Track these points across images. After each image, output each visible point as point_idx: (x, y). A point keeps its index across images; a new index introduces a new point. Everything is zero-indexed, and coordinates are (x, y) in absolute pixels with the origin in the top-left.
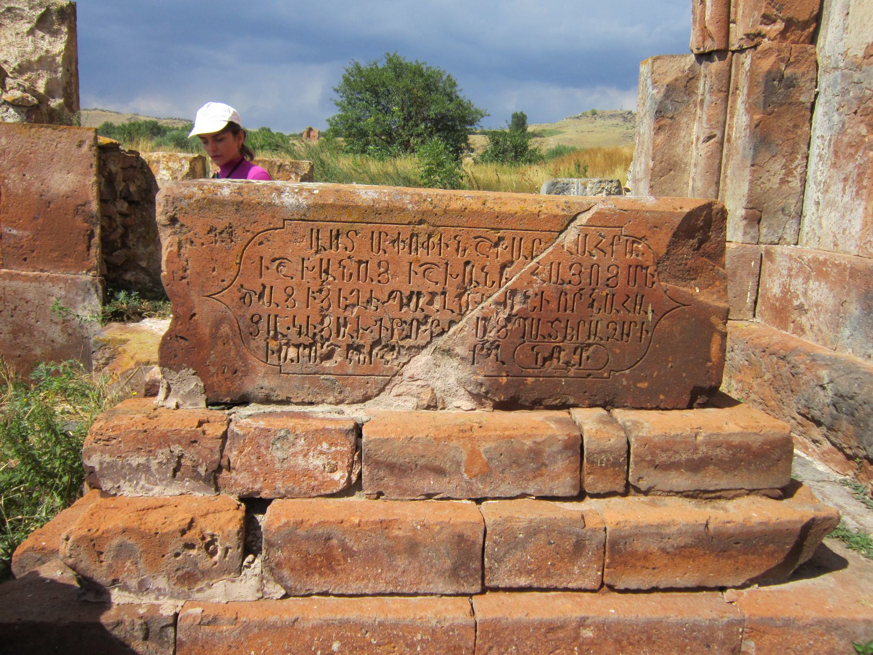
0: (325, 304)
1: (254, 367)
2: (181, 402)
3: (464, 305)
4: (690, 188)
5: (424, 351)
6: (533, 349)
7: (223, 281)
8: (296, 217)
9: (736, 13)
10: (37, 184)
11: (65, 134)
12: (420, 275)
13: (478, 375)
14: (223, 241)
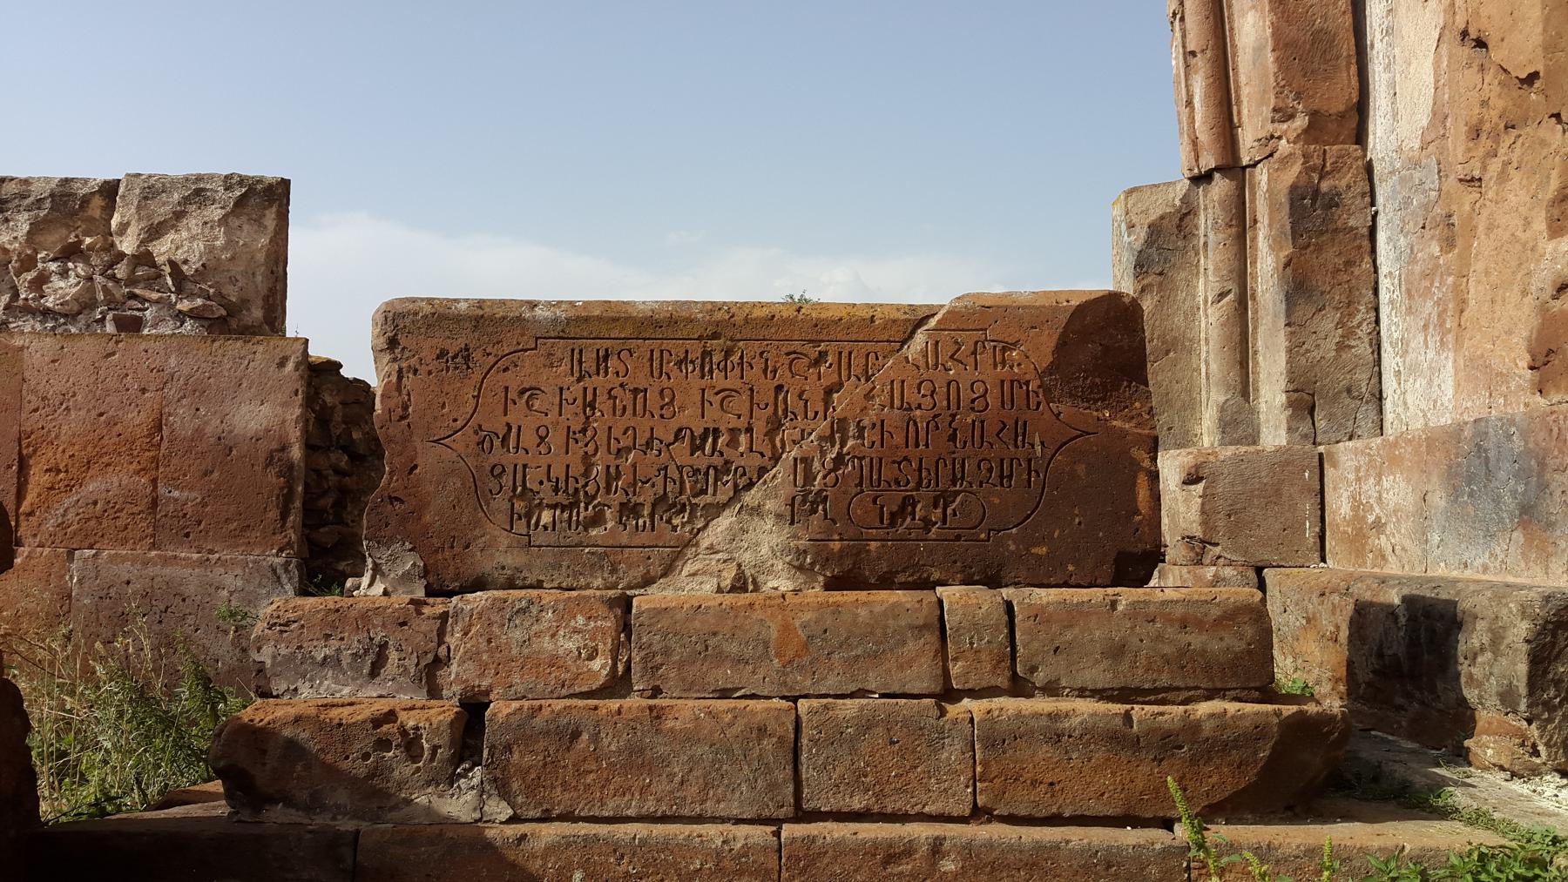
0: (591, 448)
3: (778, 444)
5: (727, 512)
6: (875, 502)
9: (1239, 113)
10: (215, 422)
11: (261, 348)
12: (716, 405)
13: (799, 539)
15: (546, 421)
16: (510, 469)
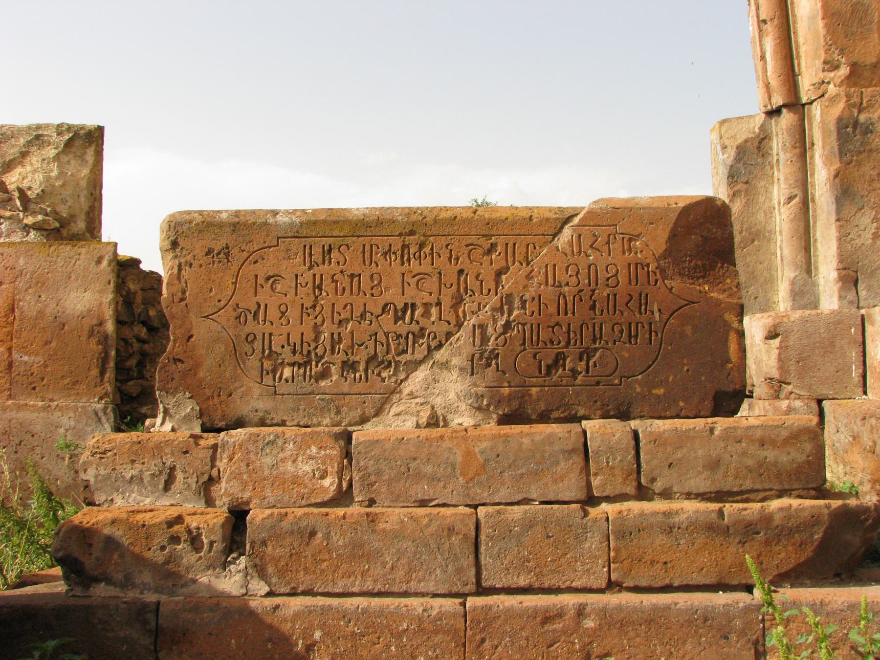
0: (319, 320)
2: (176, 427)
3: (461, 315)
4: (779, 258)
5: (423, 367)
6: (535, 357)
9: (799, 65)
10: (53, 305)
11: (84, 251)
12: (413, 286)
14: (220, 262)
16: (259, 337)
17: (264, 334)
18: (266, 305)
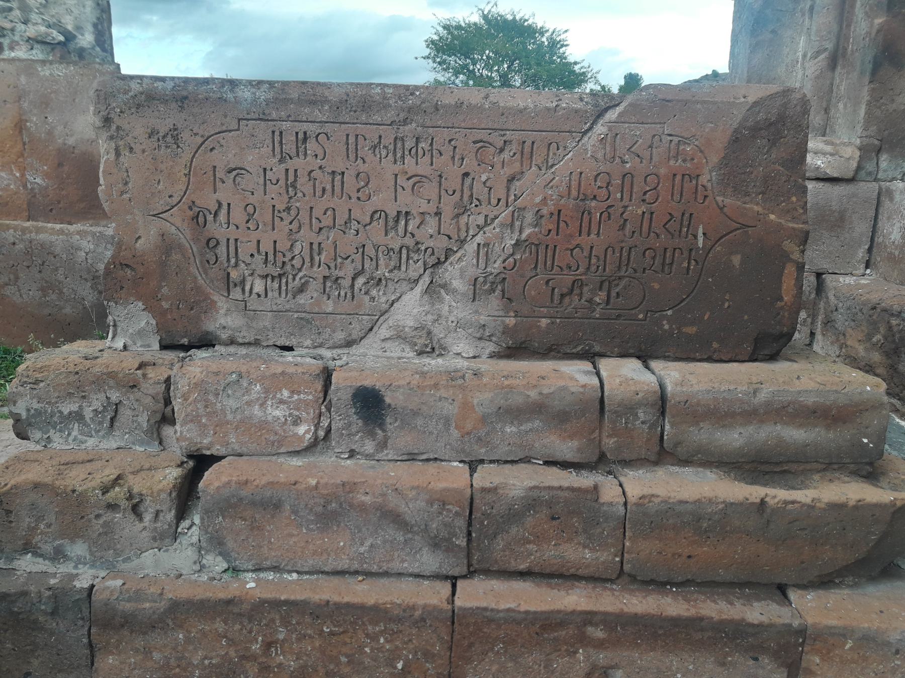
1: (214, 303)
2: (129, 343)
6: (547, 282)
7: (170, 196)
8: (252, 116)
12: (409, 190)
13: (480, 314)
15: (252, 199)
16: (223, 243)
17: (228, 240)
18: (229, 204)
